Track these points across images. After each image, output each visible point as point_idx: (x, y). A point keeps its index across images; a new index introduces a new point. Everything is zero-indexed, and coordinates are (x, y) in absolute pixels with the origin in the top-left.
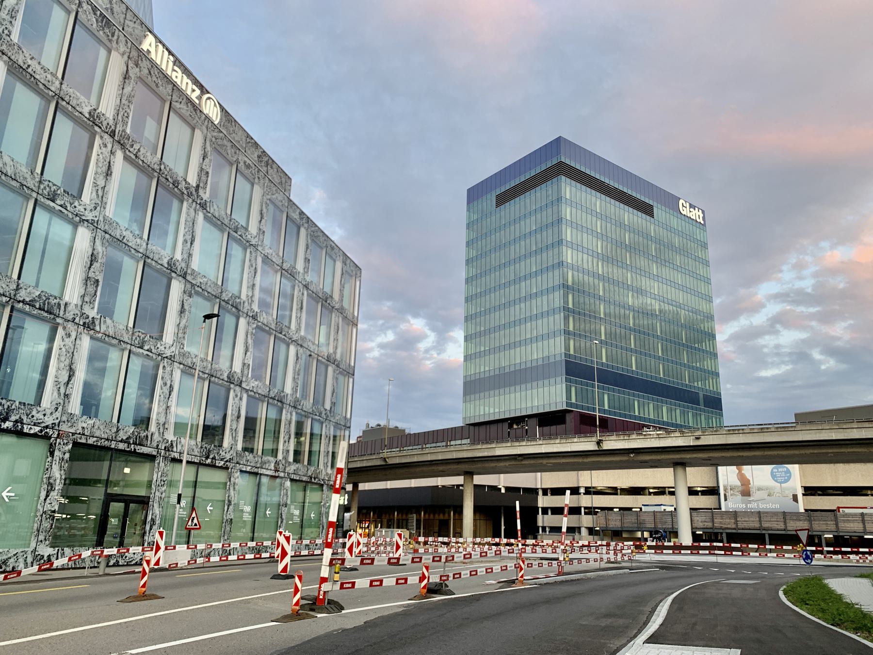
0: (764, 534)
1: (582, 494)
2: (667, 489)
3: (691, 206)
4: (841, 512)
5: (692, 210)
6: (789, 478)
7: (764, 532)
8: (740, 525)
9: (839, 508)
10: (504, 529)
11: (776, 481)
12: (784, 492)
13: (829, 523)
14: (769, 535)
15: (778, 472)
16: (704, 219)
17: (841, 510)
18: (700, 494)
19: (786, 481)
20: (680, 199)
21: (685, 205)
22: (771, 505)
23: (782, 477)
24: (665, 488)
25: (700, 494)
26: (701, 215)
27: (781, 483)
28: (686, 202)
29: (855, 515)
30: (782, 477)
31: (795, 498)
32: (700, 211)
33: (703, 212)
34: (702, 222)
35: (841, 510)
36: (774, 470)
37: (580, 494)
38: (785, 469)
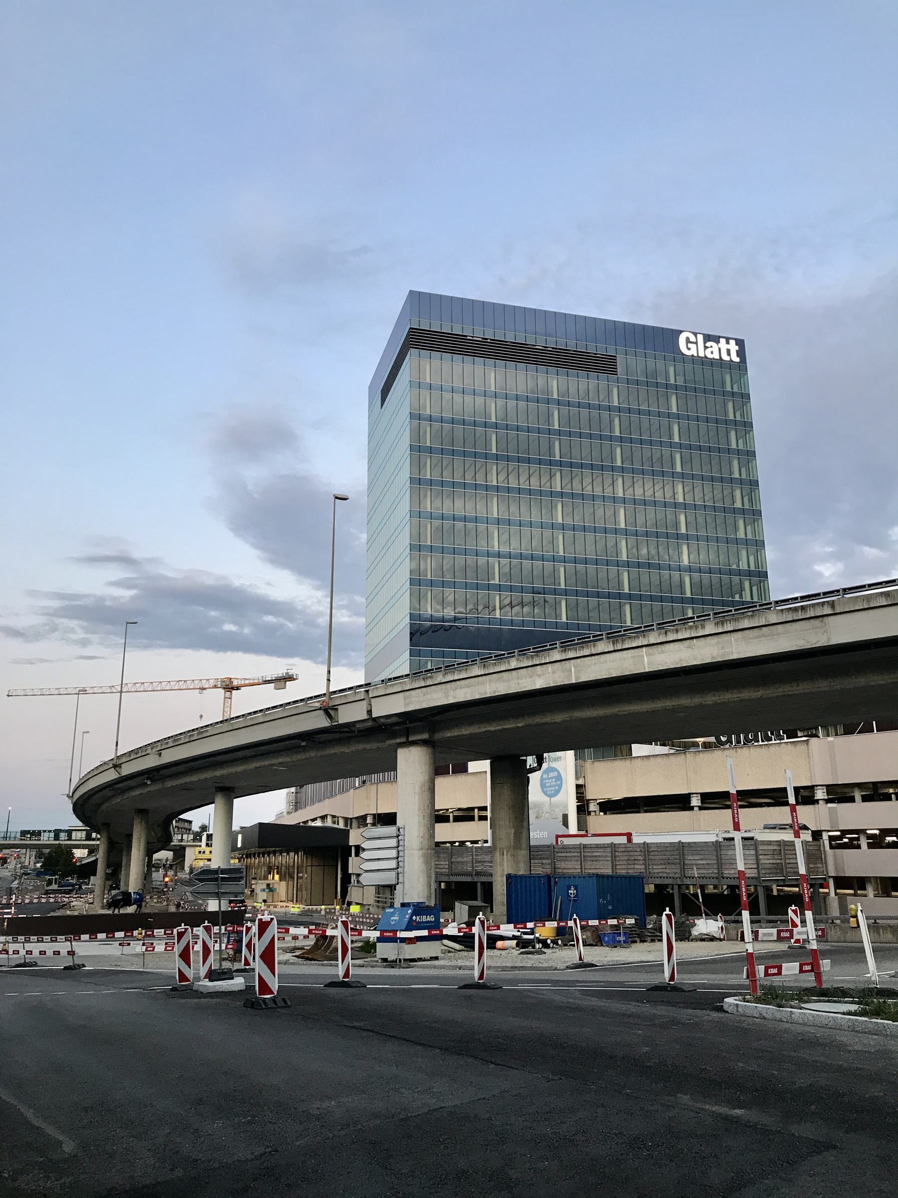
0: (476, 882)
1: (369, 825)
2: (476, 810)
3: (708, 338)
4: (559, 843)
5: (708, 344)
6: (560, 786)
7: (476, 879)
8: (459, 868)
9: (557, 837)
10: (341, 878)
11: (545, 793)
12: (553, 811)
13: (544, 861)
14: (483, 883)
15: (548, 778)
16: (741, 353)
17: (560, 839)
18: (858, 795)
19: (557, 792)
20: (681, 332)
21: (693, 338)
22: (538, 833)
23: (554, 786)
24: (472, 809)
25: (858, 795)
26: (733, 347)
27: (551, 796)
28: (695, 334)
29: (574, 847)
30: (554, 786)
31: (565, 818)
32: (730, 341)
33: (740, 343)
34: (737, 360)
35: (560, 839)
36: (544, 777)
37: (817, 802)
38: (556, 773)
